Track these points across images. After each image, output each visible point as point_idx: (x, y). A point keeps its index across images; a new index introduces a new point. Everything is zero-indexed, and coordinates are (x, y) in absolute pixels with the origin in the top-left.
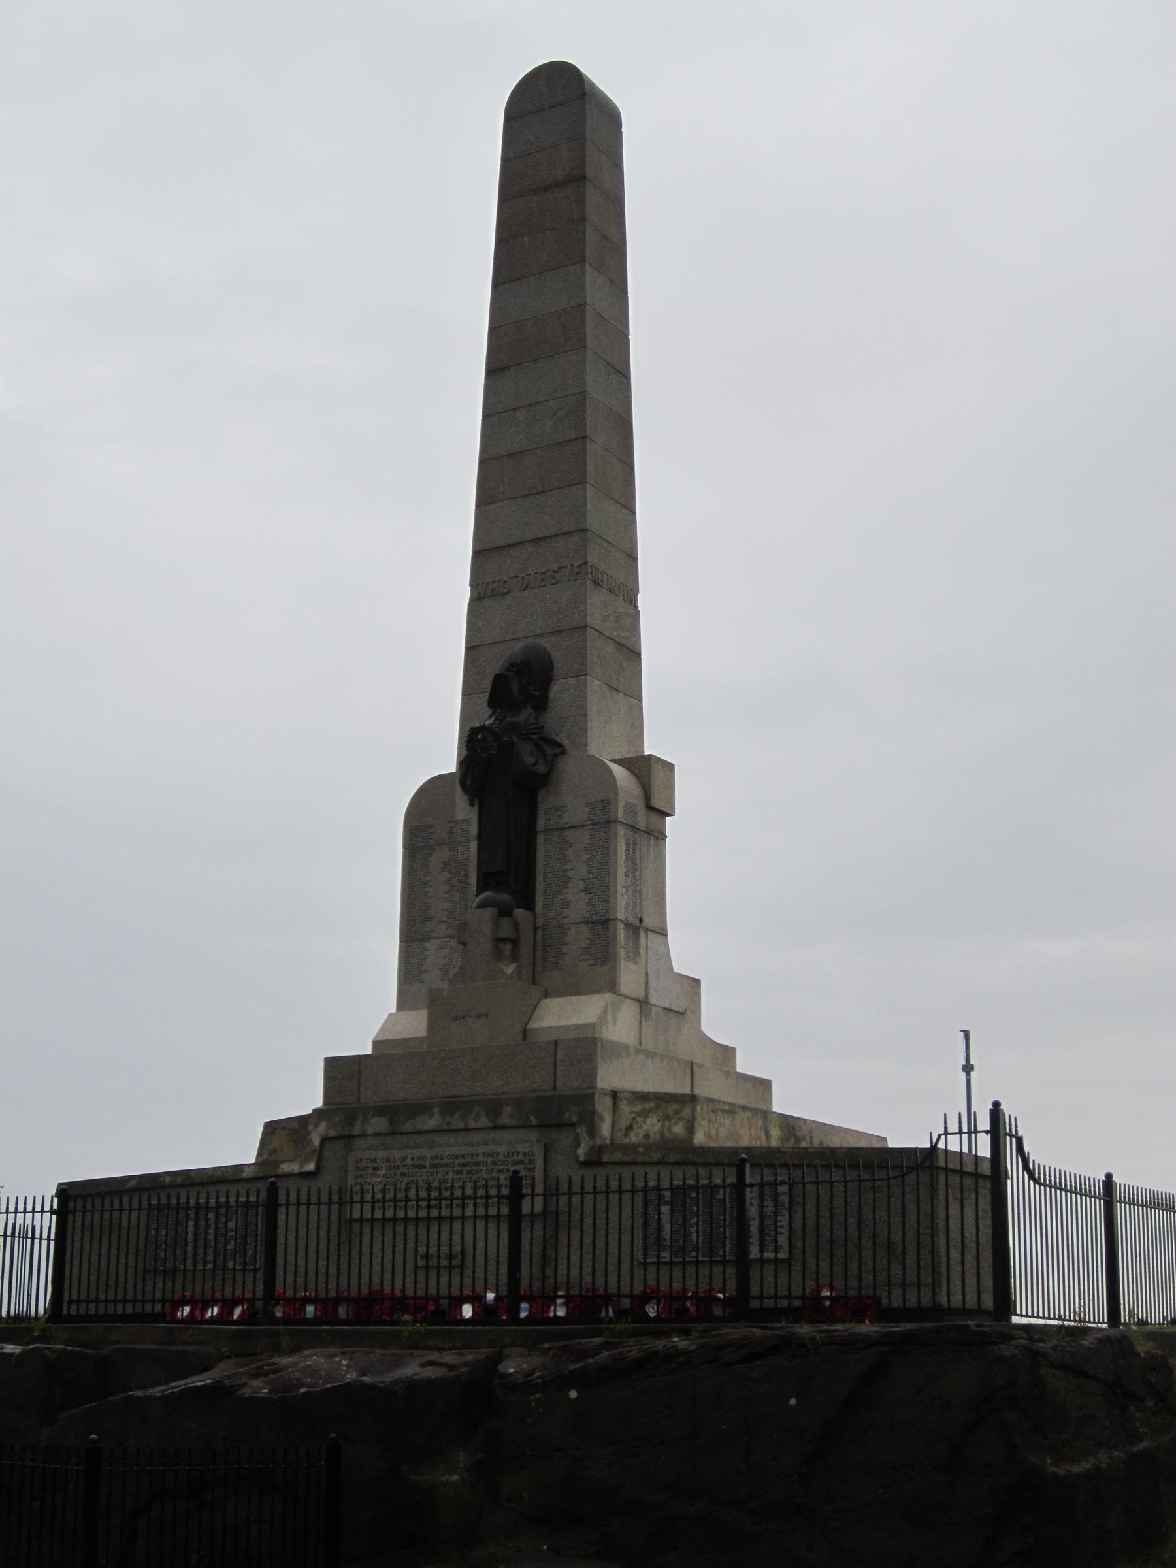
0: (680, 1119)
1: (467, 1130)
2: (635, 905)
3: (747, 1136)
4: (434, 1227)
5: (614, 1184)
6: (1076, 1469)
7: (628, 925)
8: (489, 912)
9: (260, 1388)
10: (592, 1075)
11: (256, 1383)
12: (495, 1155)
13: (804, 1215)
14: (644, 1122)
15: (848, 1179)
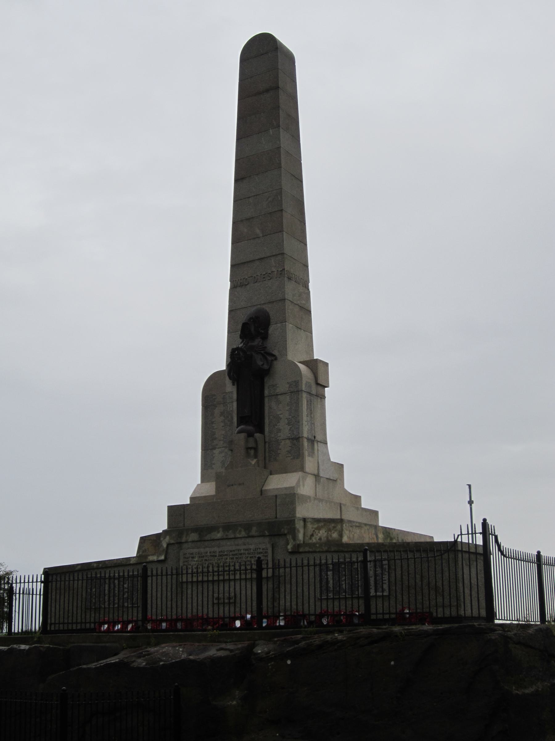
0: (336, 531)
1: (236, 538)
2: (312, 430)
3: (367, 538)
5: (305, 562)
6: (527, 691)
7: (308, 439)
8: (243, 435)
9: (141, 663)
10: (294, 510)
11: (139, 660)
12: (249, 550)
13: (395, 574)
14: (319, 532)
15: (416, 557)
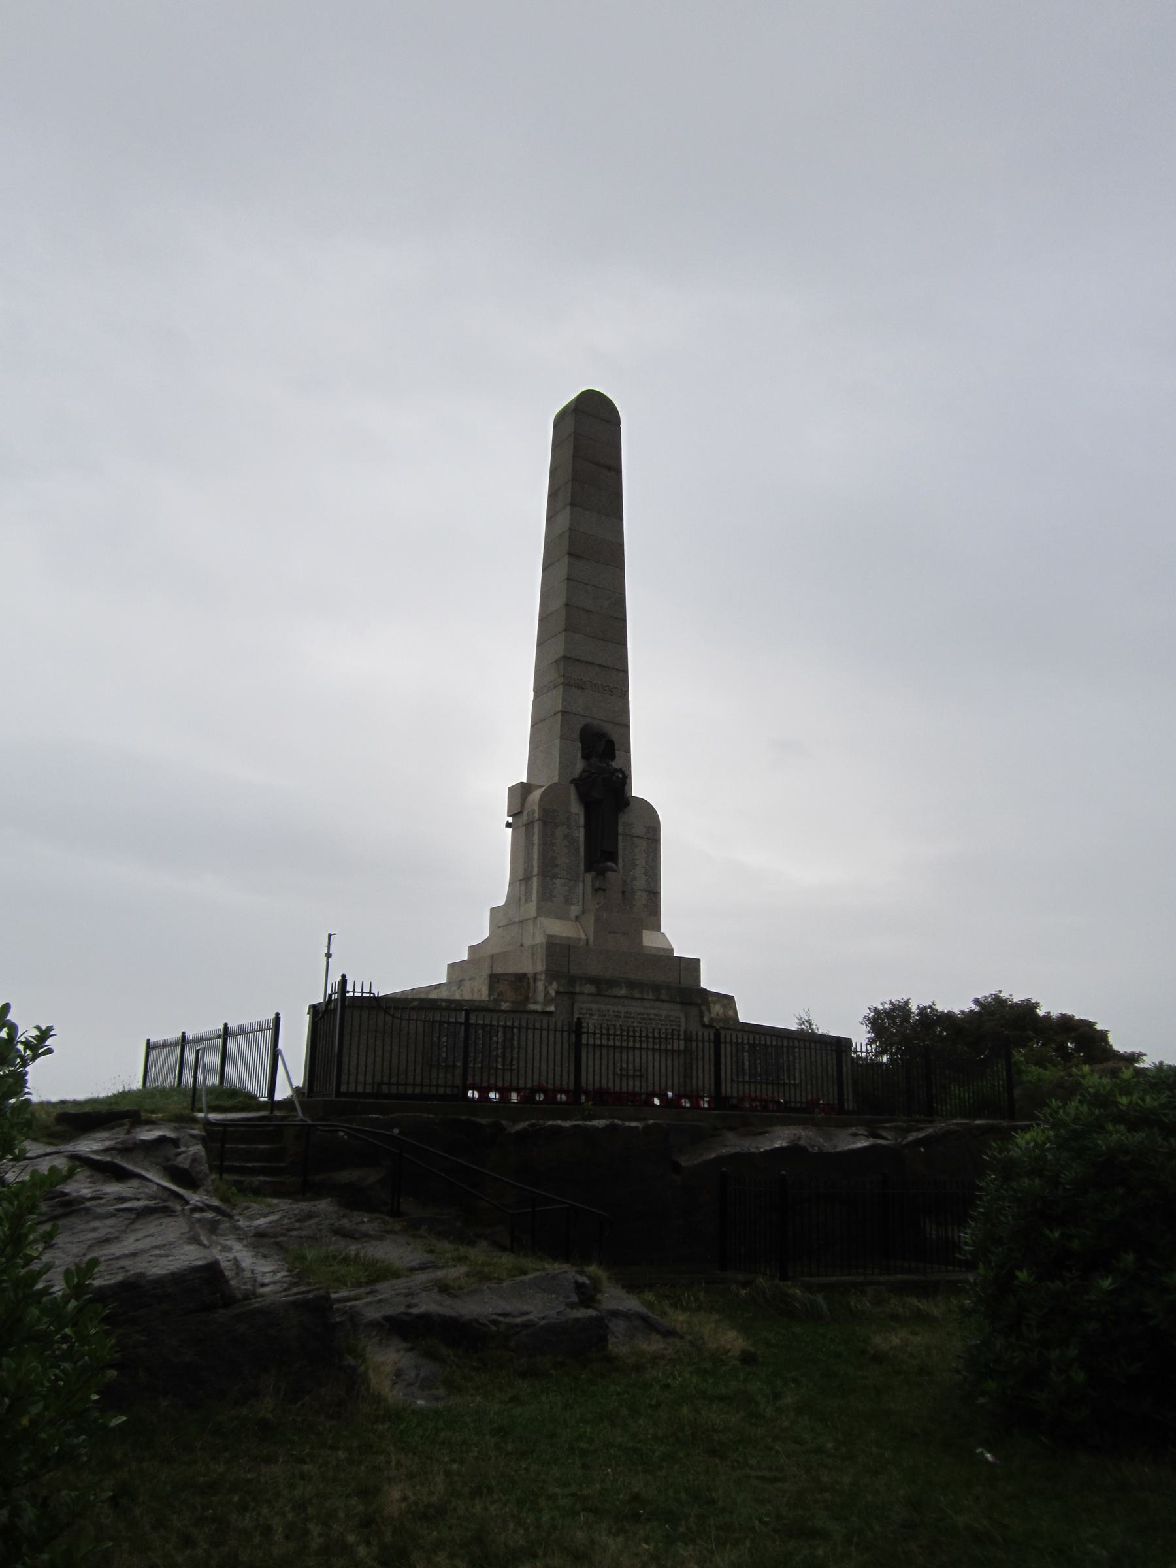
1: (642, 999)
4: (624, 1052)
